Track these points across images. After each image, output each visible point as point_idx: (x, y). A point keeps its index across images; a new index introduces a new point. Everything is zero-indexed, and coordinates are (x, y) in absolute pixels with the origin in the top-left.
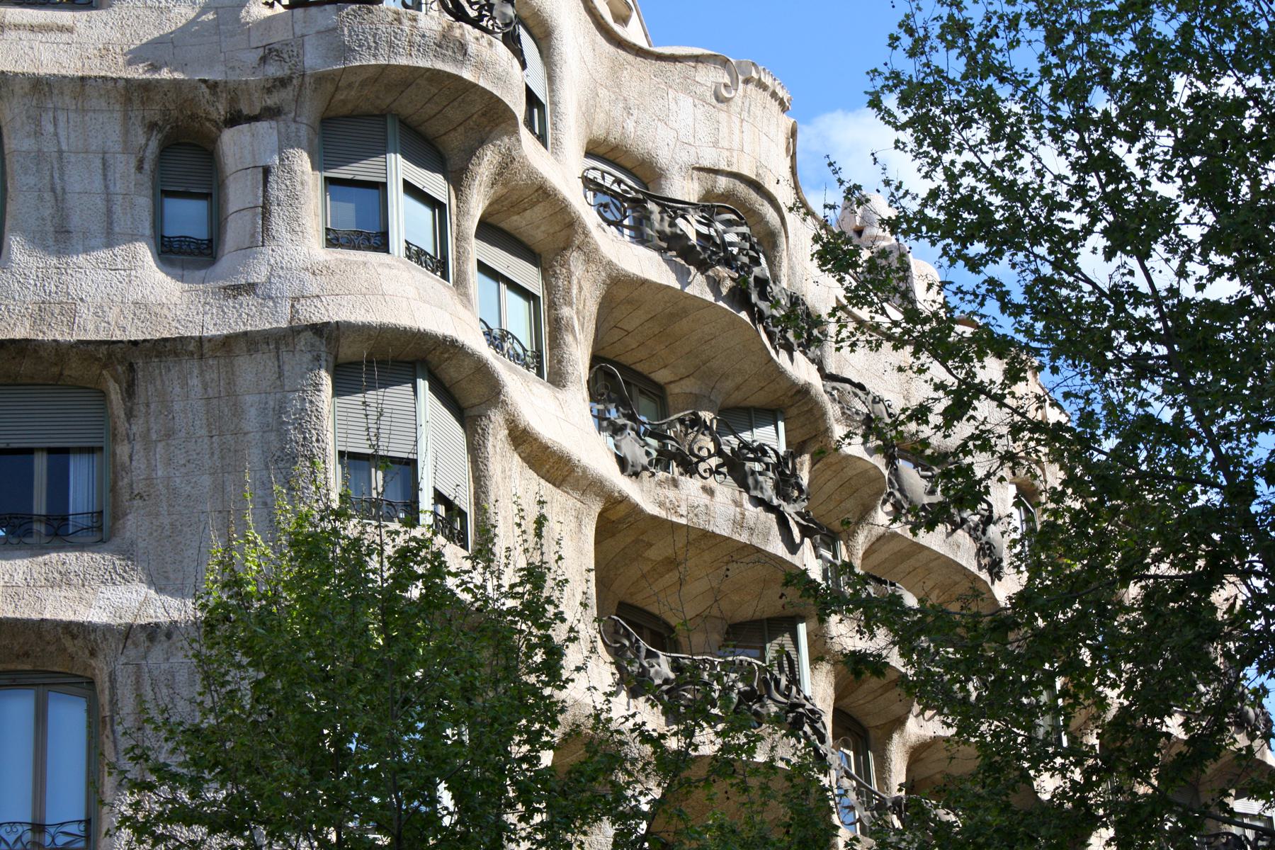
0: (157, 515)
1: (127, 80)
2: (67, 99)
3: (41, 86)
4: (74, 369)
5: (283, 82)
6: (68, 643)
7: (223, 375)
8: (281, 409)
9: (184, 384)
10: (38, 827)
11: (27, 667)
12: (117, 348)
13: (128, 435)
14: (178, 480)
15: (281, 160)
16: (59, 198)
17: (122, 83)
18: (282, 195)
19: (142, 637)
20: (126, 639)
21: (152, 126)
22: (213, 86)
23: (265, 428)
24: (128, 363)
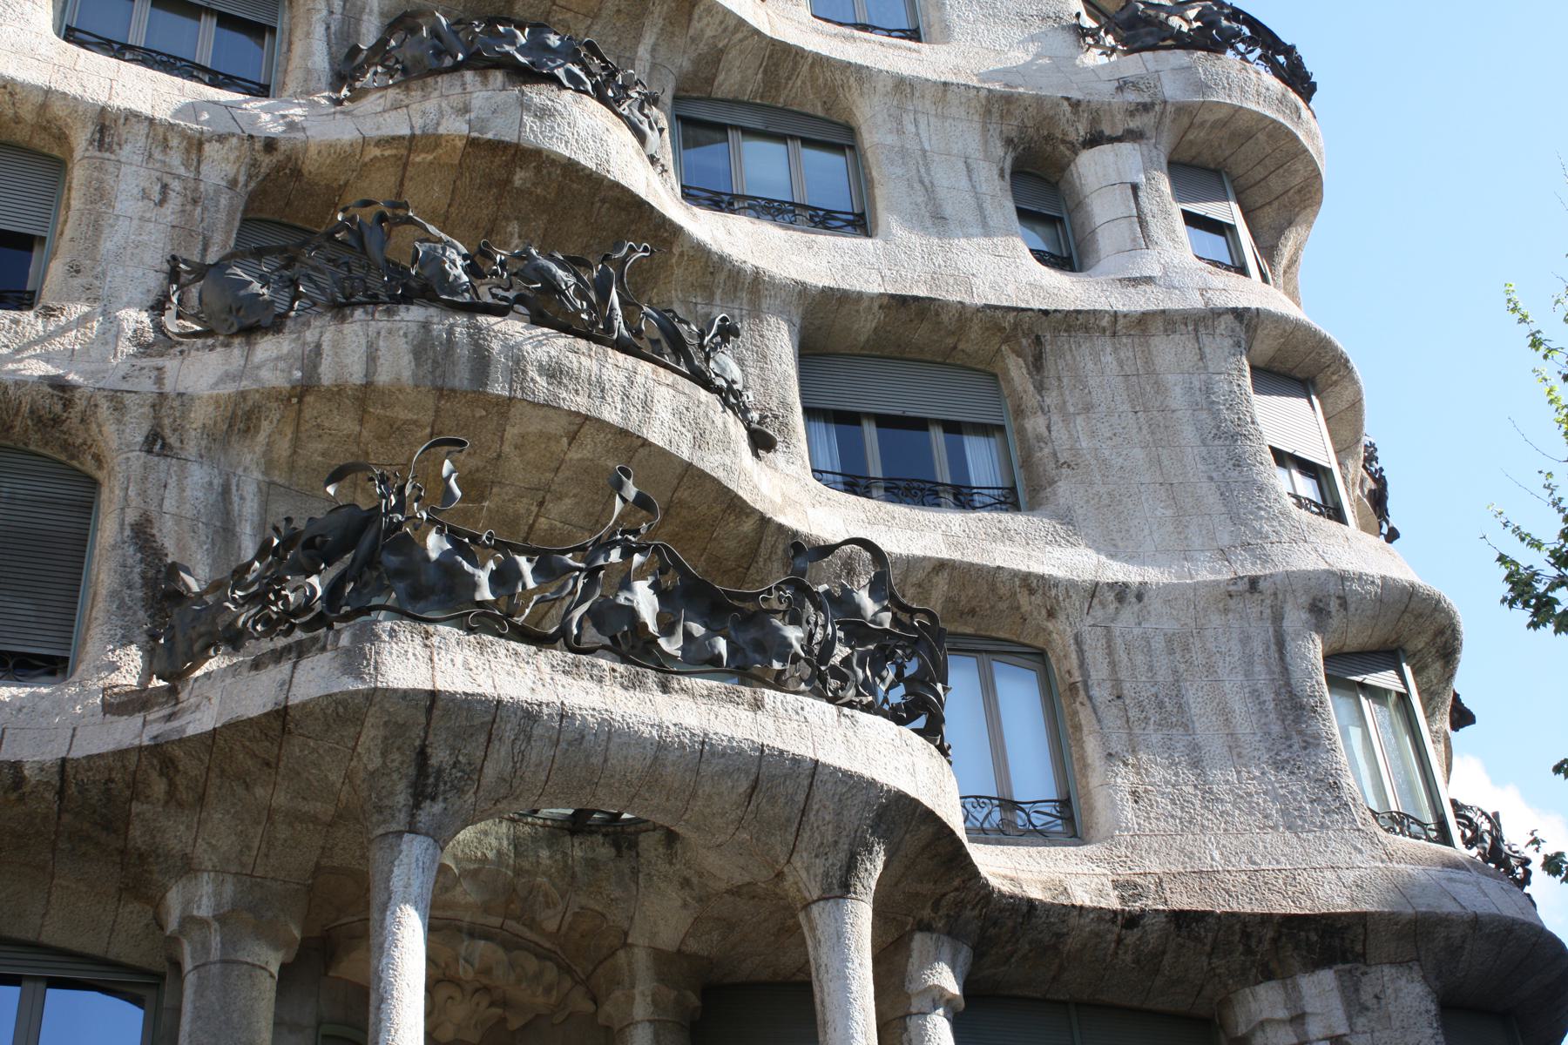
0: (1091, 484)
1: (989, 90)
2: (927, 102)
3: (903, 86)
4: (973, 340)
5: (1146, 108)
6: (1023, 599)
7: (1139, 354)
8: (1208, 390)
9: (1097, 361)
10: (1009, 805)
11: (969, 630)
12: (1026, 316)
13: (1042, 409)
14: (1107, 453)
15: (1148, 179)
16: (930, 190)
17: (983, 93)
18: (1155, 209)
19: (1111, 597)
20: (1093, 597)
21: (1009, 142)
22: (1075, 105)
23: (1195, 407)
24: (1033, 333)
